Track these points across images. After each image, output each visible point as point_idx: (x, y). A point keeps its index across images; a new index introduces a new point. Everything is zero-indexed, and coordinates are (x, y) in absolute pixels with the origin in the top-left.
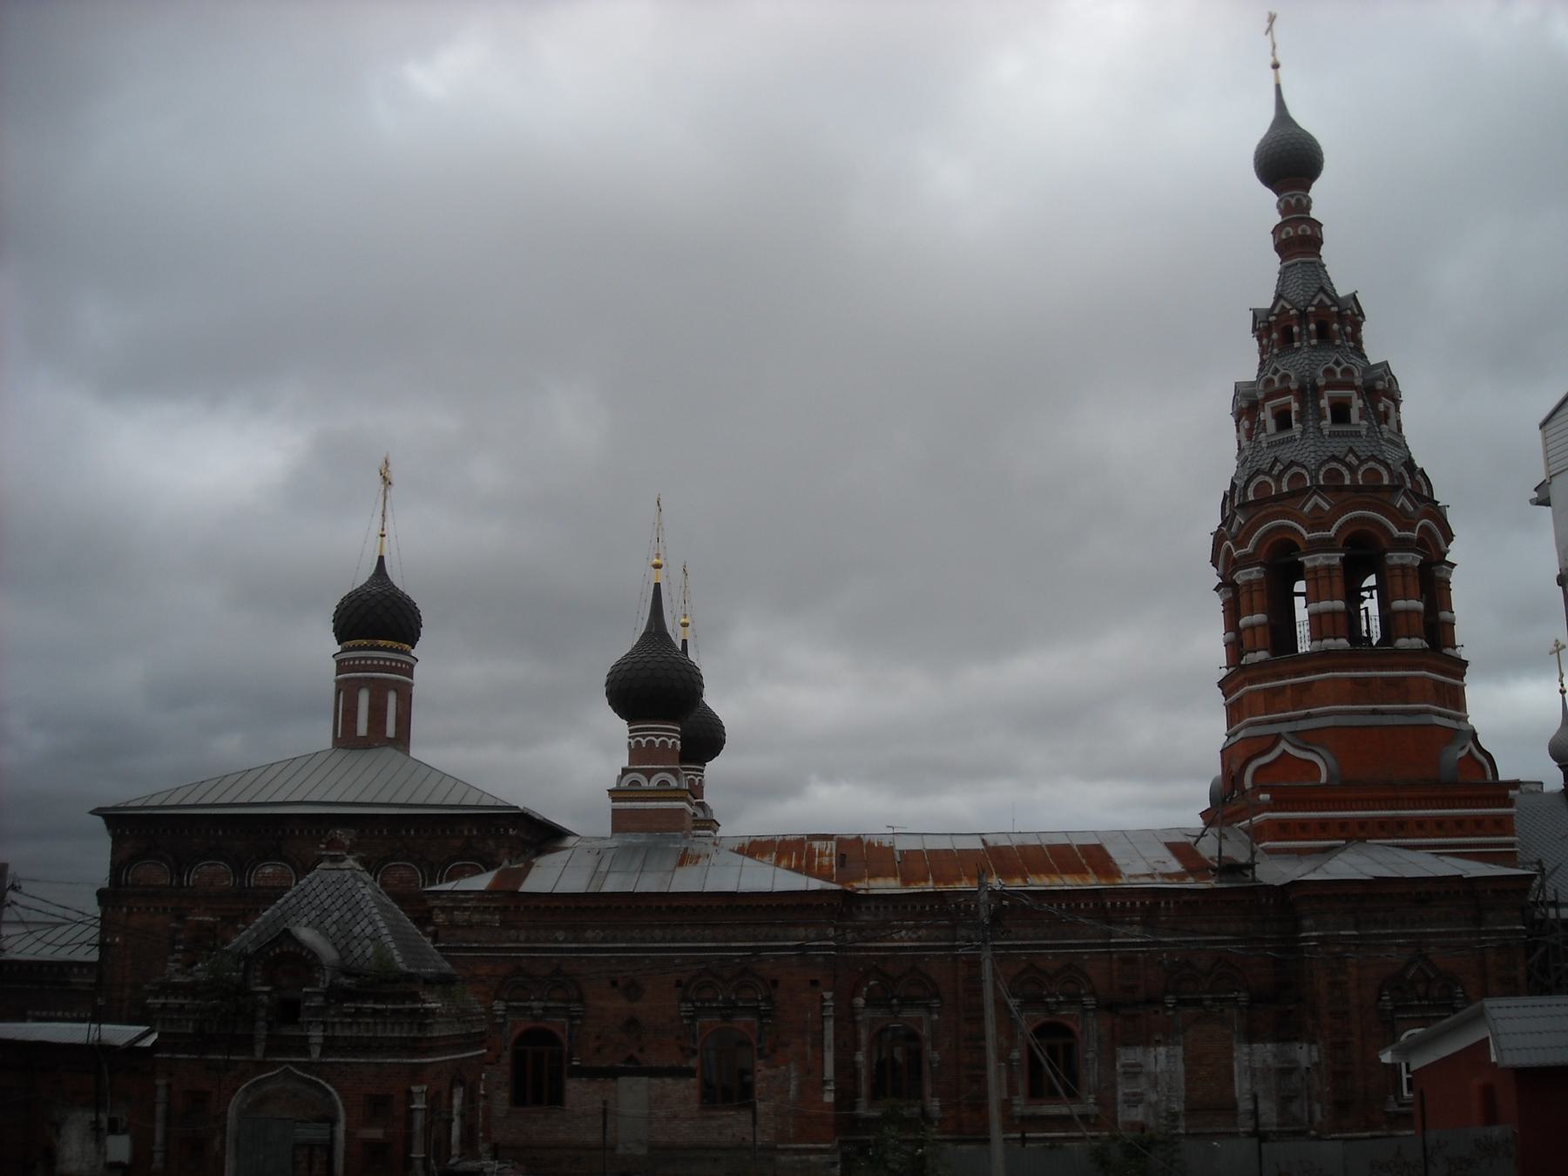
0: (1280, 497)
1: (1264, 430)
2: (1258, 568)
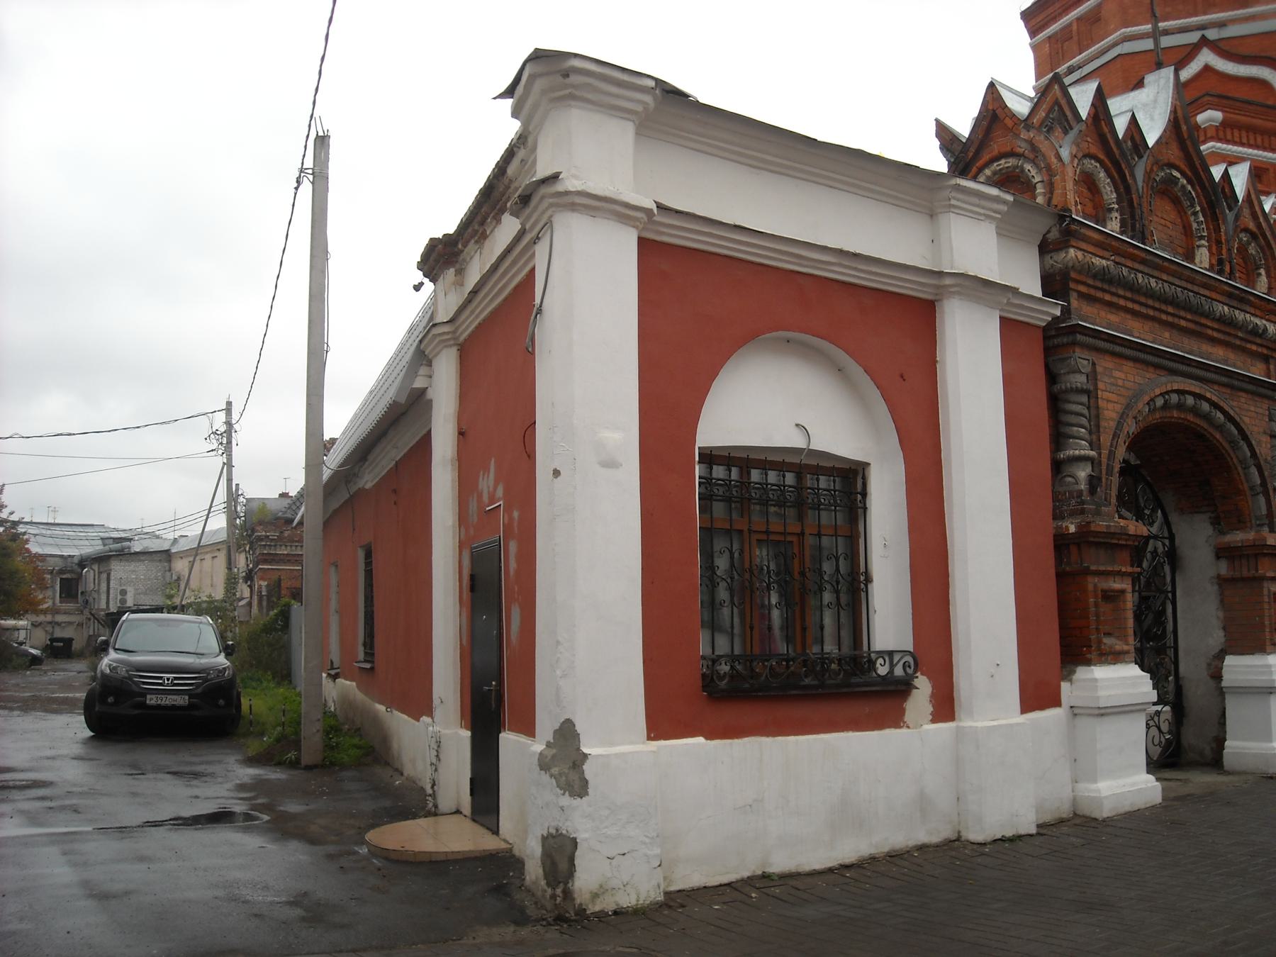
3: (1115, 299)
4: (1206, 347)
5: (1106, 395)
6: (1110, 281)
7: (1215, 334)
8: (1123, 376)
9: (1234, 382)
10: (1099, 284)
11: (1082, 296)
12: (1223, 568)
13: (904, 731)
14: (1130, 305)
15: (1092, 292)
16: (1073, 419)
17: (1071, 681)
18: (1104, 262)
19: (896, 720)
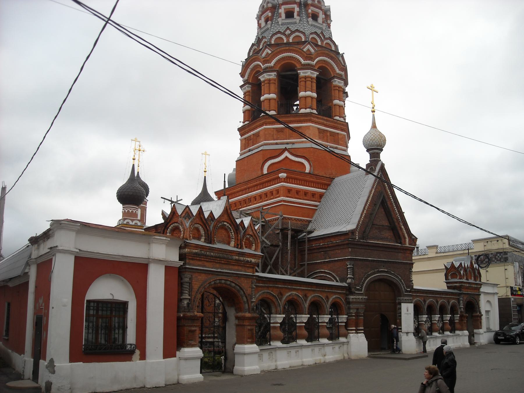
0: (288, 44)
1: (281, 17)
2: (276, 73)
3: (201, 259)
4: (231, 267)
5: (195, 283)
6: (199, 255)
7: (234, 263)
8: (201, 277)
9: (239, 276)
10: (195, 256)
11: (189, 259)
12: (237, 322)
13: (132, 362)
14: (205, 259)
15: (193, 258)
16: (185, 289)
17: (180, 351)
18: (197, 251)
19: (130, 360)
